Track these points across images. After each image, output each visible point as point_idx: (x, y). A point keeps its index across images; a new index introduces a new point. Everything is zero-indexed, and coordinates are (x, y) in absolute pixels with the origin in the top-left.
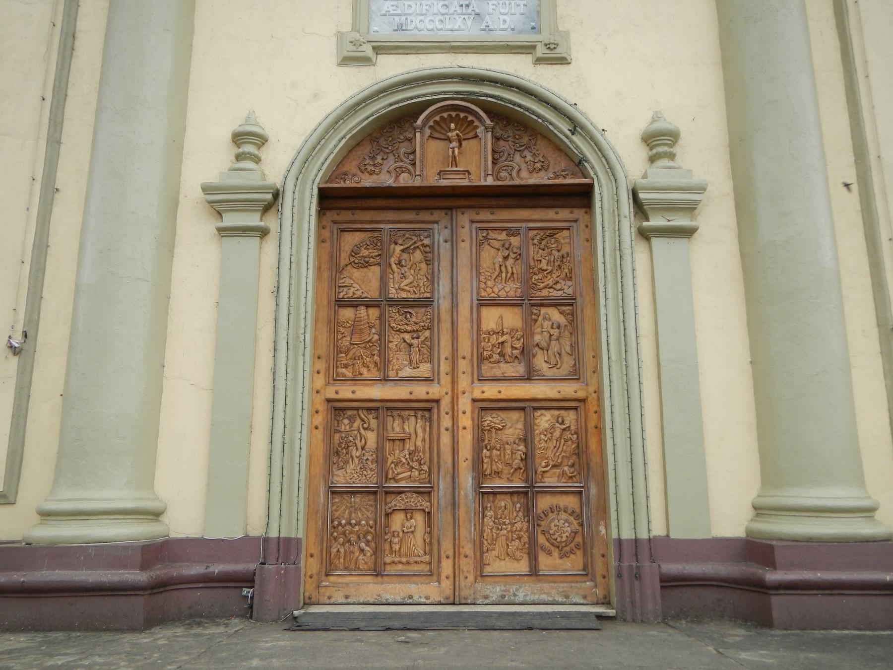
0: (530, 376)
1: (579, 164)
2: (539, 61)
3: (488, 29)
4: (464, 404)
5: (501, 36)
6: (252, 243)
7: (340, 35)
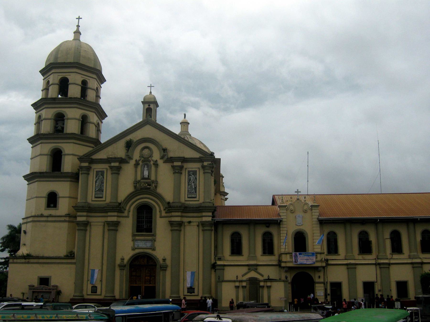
0: (150, 284)
1: (155, 263)
2: (152, 250)
3: (147, 246)
4: (144, 286)
5: (148, 247)
6: (123, 270)
7: (132, 246)
